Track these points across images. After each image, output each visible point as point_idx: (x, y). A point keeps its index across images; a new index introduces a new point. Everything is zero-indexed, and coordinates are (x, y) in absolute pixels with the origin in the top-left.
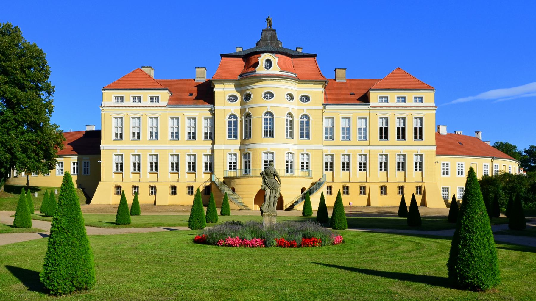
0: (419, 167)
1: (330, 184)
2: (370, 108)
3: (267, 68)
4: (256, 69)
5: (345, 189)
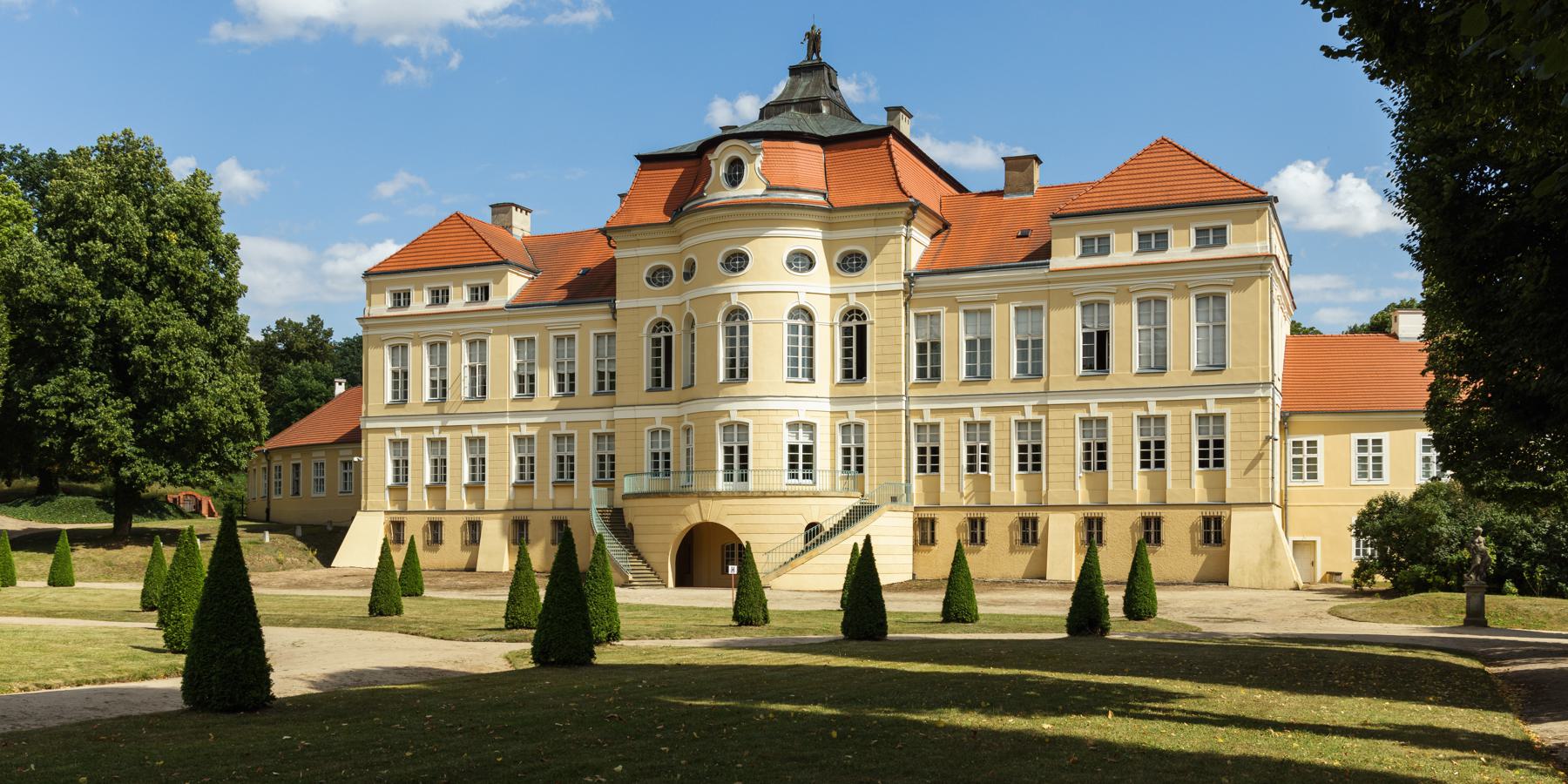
5: (976, 527)
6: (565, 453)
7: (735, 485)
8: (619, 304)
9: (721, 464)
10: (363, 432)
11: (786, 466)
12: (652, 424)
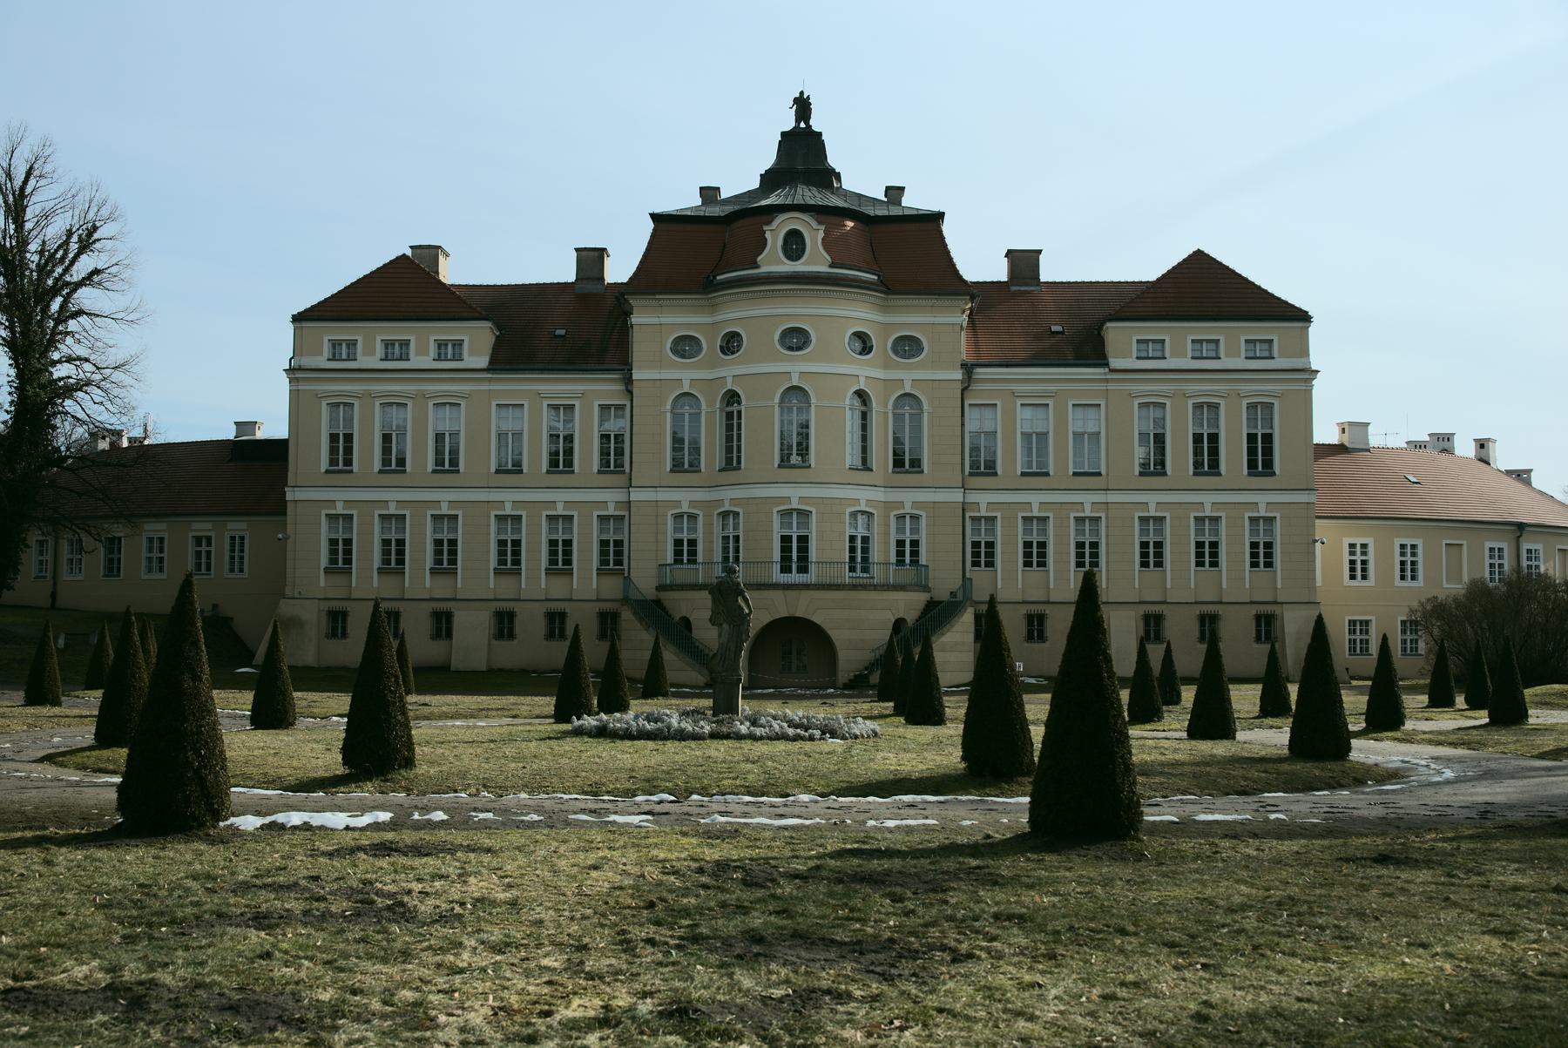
0: (1262, 555)
4: (759, 259)
6: (685, 536)
7: (794, 577)
9: (777, 556)
10: (288, 504)
11: (847, 560)
12: (677, 508)
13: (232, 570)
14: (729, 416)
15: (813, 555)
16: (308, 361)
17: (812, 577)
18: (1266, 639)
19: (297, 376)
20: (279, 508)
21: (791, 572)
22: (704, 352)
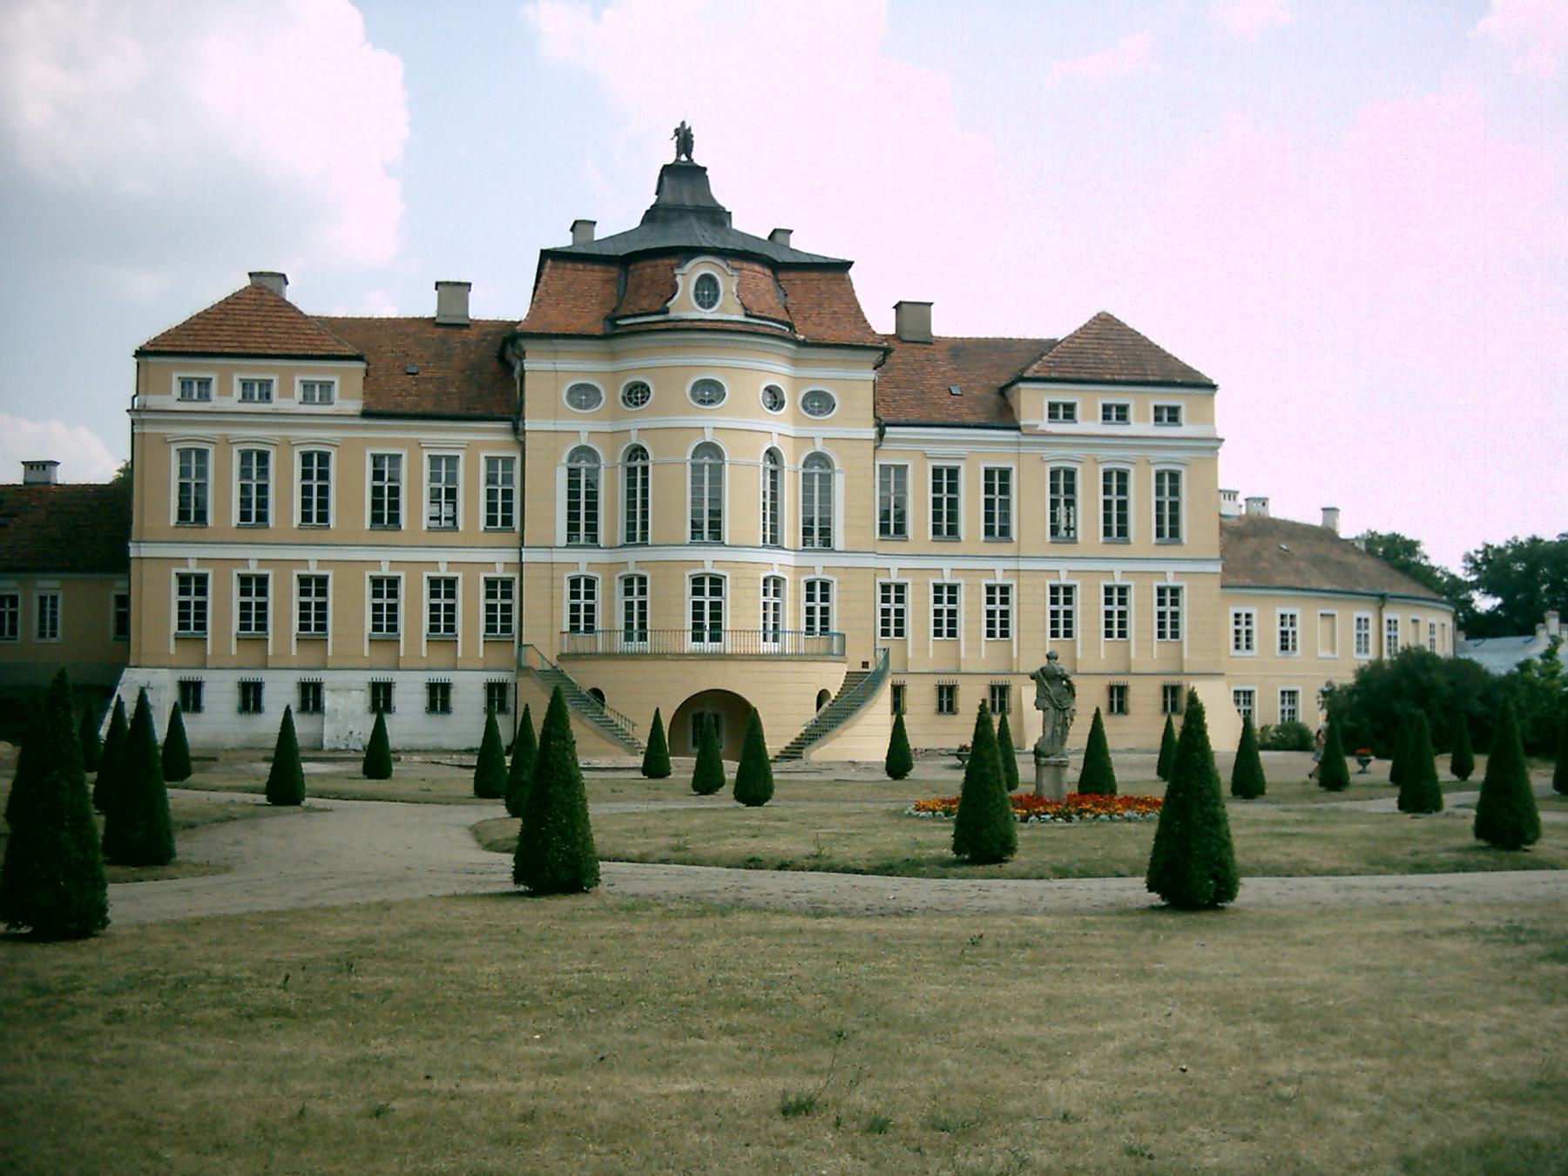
0: (1169, 626)
1: (899, 680)
2: (1023, 439)
3: (701, 304)
7: (708, 646)
8: (529, 425)
9: (689, 623)
10: (133, 563)
13: (42, 635)
14: (631, 471)
15: (727, 622)
16: (154, 401)
17: (647, 646)
18: (1118, 710)
19: (143, 417)
20: (121, 564)
21: (702, 640)
22: (603, 401)
